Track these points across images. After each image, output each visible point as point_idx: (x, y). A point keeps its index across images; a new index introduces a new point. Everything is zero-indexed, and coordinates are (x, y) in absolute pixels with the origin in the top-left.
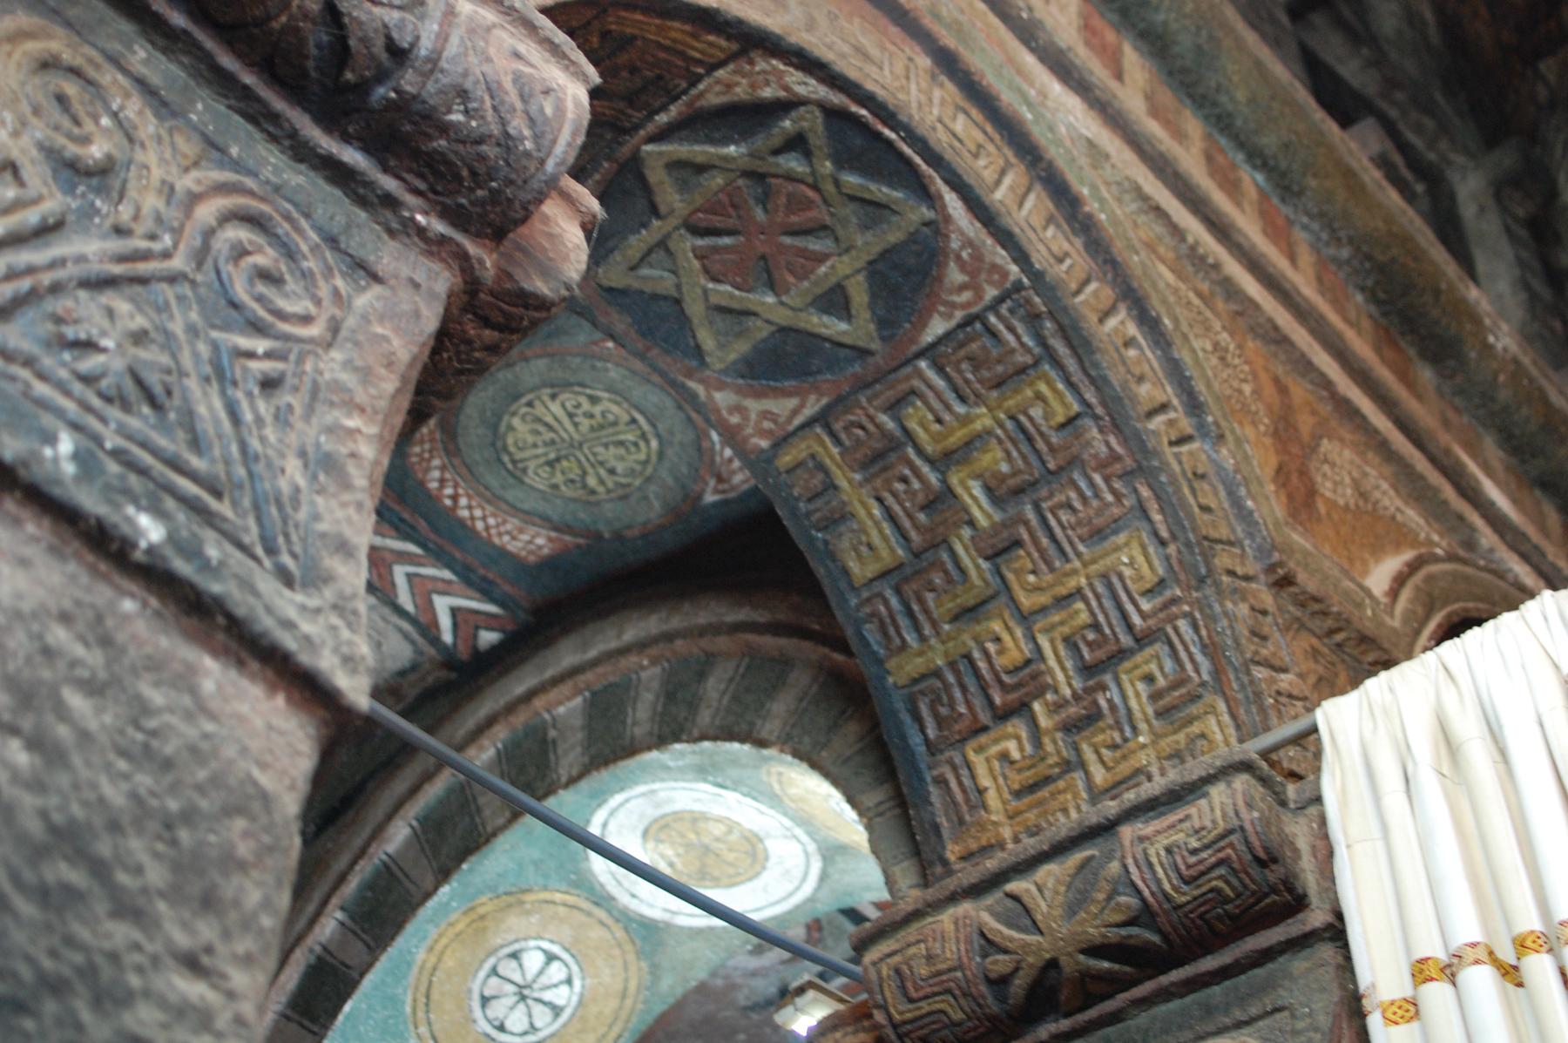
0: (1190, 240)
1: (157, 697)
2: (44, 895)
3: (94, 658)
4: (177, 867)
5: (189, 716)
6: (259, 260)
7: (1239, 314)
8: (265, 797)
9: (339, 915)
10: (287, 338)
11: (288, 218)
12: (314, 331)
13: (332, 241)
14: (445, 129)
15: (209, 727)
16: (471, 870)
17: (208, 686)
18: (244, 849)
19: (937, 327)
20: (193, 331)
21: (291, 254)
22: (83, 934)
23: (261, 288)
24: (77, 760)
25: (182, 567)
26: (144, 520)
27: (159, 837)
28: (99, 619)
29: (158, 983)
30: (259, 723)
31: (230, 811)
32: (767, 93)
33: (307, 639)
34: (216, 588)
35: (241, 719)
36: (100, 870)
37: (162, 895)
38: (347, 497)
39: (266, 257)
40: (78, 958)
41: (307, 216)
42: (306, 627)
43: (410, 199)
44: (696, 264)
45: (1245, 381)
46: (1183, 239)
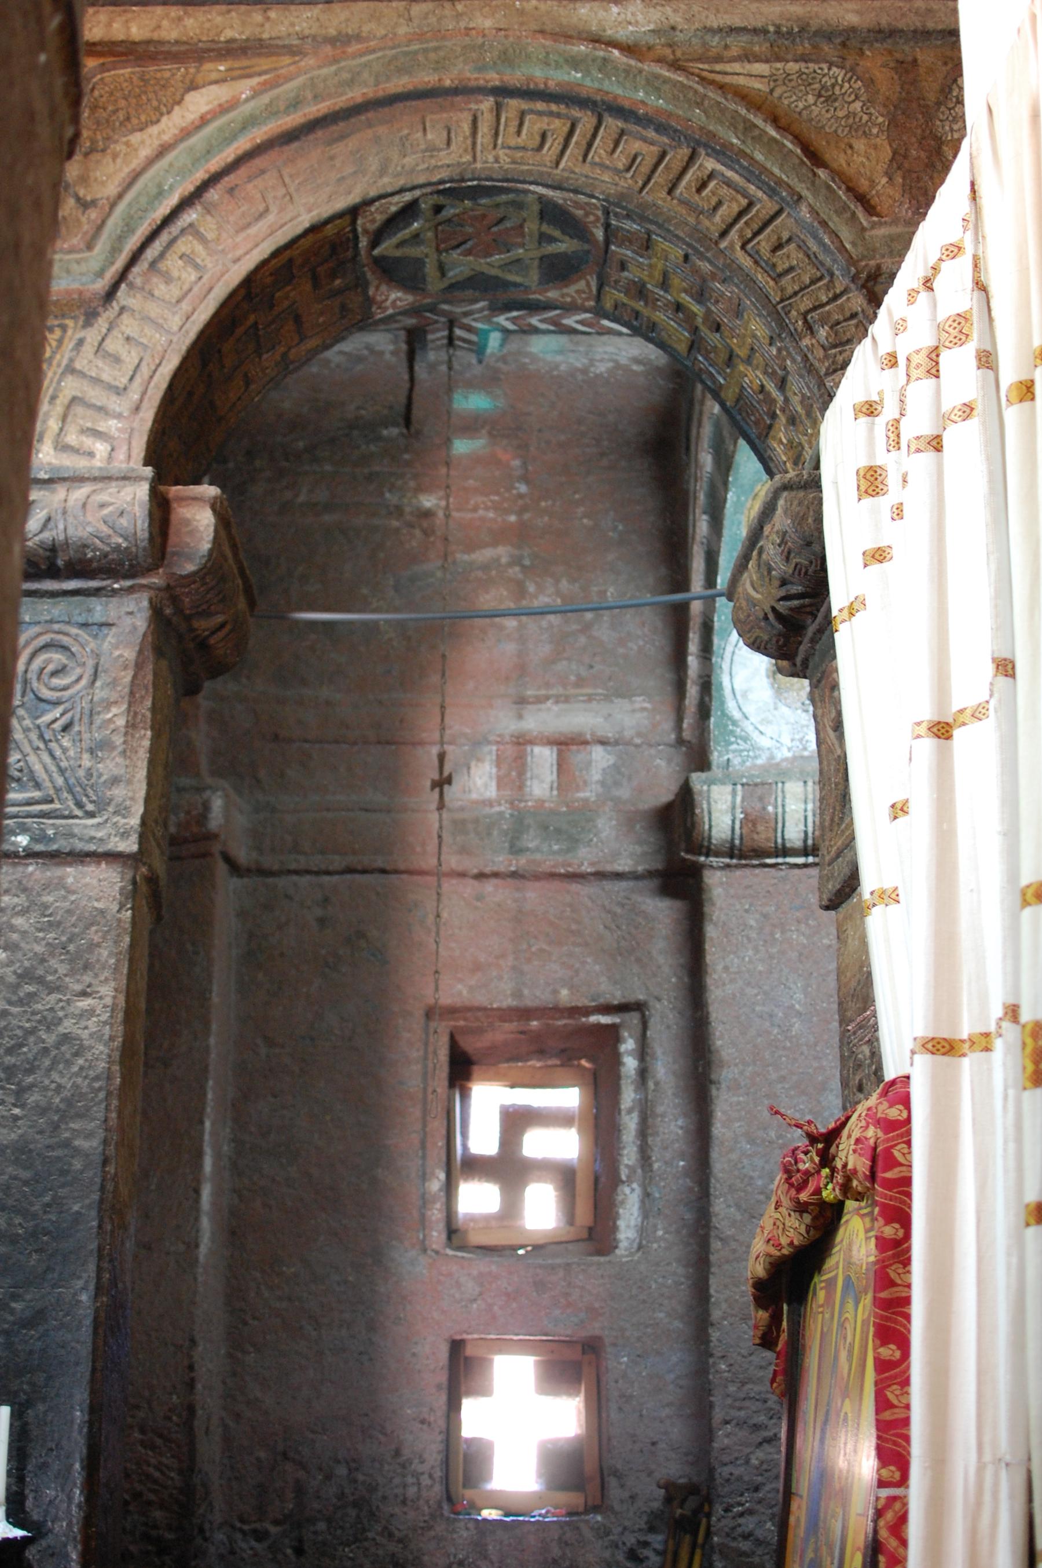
0: (772, 29)
1: (51, 899)
2: (21, 1002)
3: (21, 900)
4: (71, 961)
5: (65, 898)
6: (51, 668)
7: (844, 44)
8: (102, 912)
9: (705, 517)
10: (71, 697)
11: (59, 633)
12: (84, 682)
13: (85, 625)
14: (91, 560)
15: (73, 898)
16: (736, 479)
17: (70, 880)
18: (97, 939)
19: (599, 234)
20: (27, 730)
21: (65, 648)
22: (39, 1007)
23: (56, 682)
24: (23, 945)
25: (39, 847)
26: (19, 838)
27: (61, 954)
28: (20, 882)
29: (71, 1009)
30: (95, 882)
31: (87, 927)
32: (393, 209)
33: (101, 840)
34: (55, 847)
35: (86, 885)
36: (41, 980)
37: (66, 975)
38: (115, 753)
39: (57, 658)
40: (38, 1017)
41: (68, 623)
42: (99, 834)
43: (108, 582)
44: (471, 258)
45: (857, 98)
46: (765, 32)
